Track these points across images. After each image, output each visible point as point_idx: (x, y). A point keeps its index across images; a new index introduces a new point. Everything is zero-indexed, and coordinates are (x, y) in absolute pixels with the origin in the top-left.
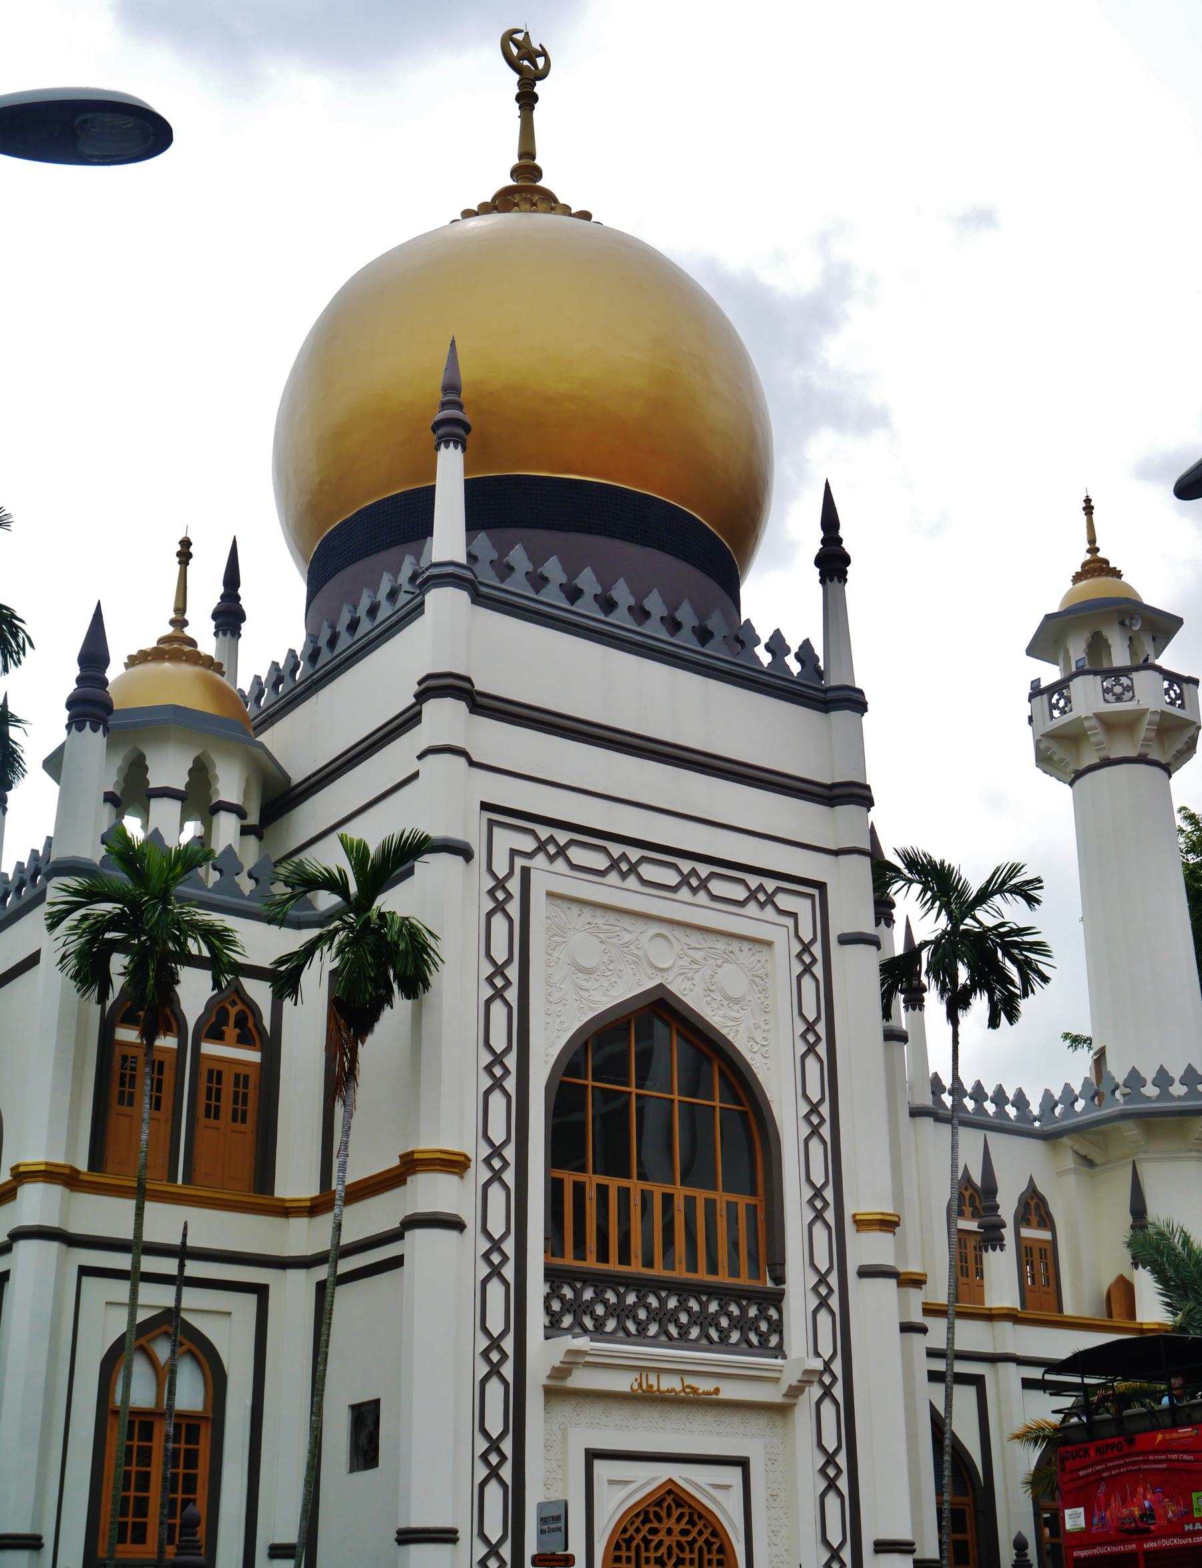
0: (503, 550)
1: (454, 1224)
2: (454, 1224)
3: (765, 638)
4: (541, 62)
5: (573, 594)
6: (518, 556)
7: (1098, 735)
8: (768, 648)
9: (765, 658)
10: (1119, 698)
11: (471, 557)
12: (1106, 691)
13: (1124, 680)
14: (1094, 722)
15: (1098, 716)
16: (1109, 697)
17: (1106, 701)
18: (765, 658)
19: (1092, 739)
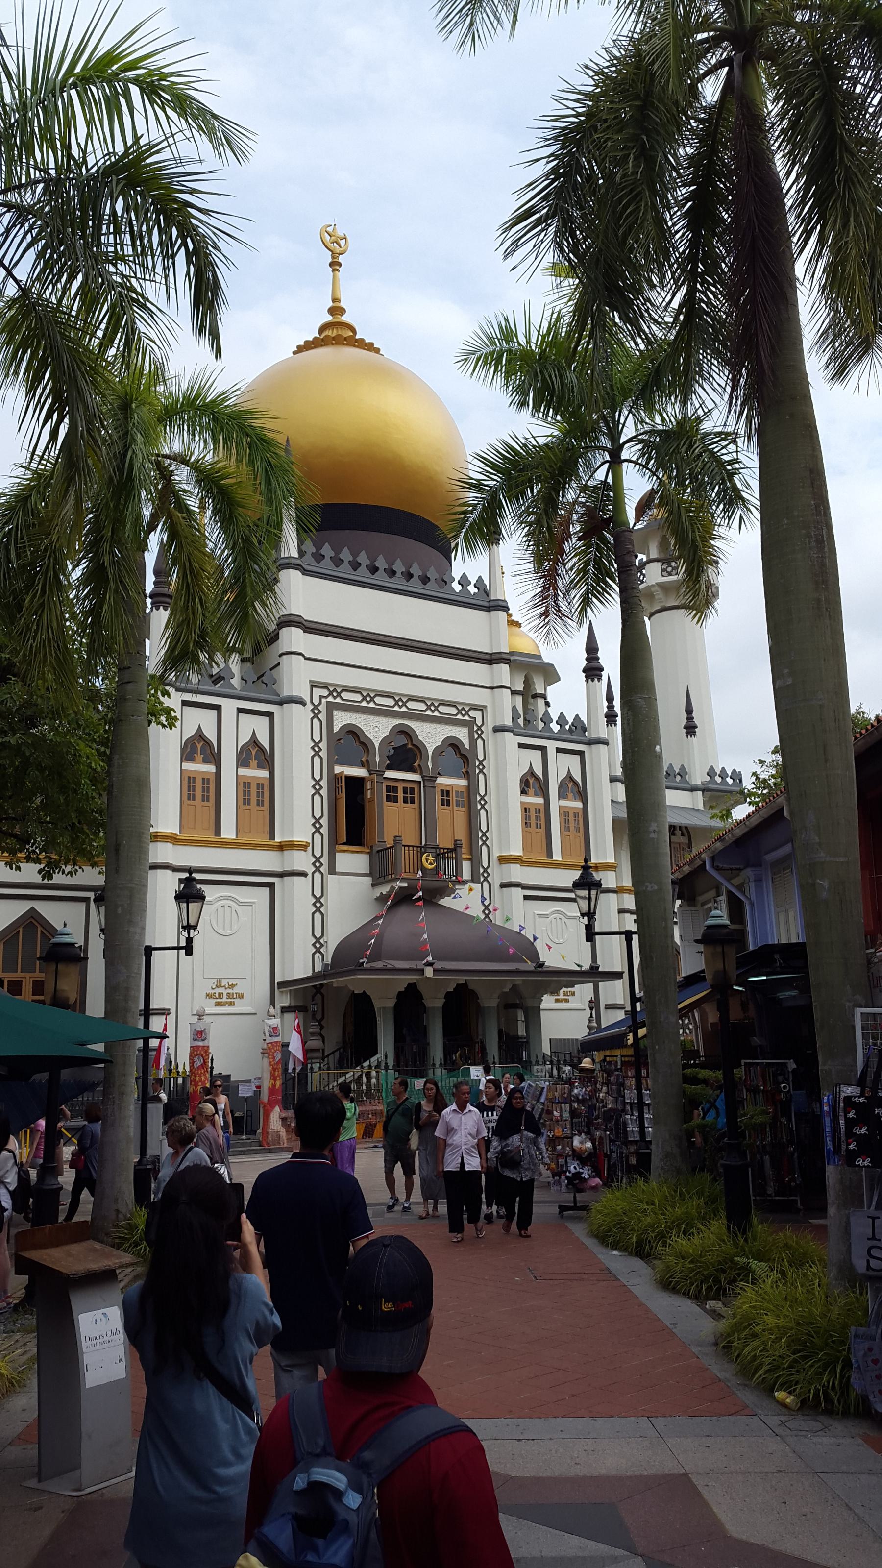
0: (318, 547)
1: (304, 874)
2: (304, 874)
3: (457, 578)
4: (342, 242)
5: (355, 566)
6: (327, 550)
7: (659, 594)
8: (459, 583)
9: (457, 588)
10: (670, 574)
11: (301, 553)
12: (663, 570)
13: (673, 564)
14: (657, 588)
15: (660, 585)
16: (665, 573)
17: (663, 576)
18: (457, 588)
19: (656, 597)
